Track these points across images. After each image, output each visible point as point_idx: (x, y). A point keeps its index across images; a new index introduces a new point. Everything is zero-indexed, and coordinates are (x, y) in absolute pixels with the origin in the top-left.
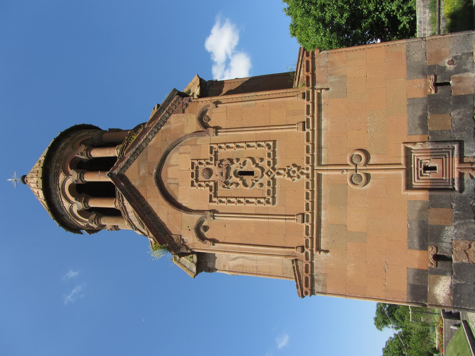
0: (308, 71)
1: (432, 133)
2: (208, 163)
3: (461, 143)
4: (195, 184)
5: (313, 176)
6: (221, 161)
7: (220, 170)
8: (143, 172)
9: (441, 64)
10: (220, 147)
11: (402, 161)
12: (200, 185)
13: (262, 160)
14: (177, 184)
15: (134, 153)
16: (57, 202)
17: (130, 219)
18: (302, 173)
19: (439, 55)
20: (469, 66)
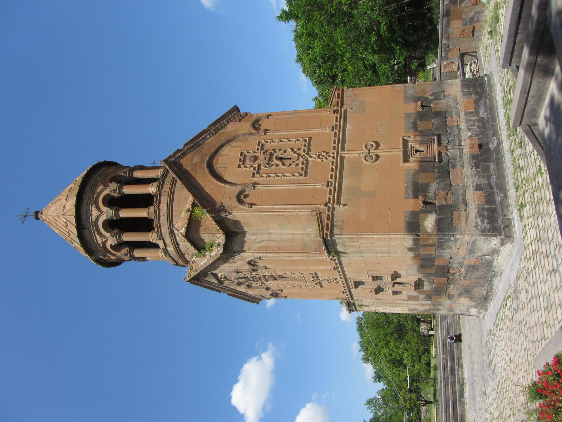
0: (338, 98)
1: (420, 131)
2: (254, 152)
3: (439, 137)
4: (242, 166)
5: (337, 158)
6: (266, 151)
7: (265, 156)
8: (196, 160)
9: (425, 96)
10: (266, 142)
11: (401, 146)
12: (245, 167)
13: (299, 149)
14: (226, 167)
15: (191, 147)
16: (85, 212)
17: (160, 224)
18: (329, 156)
19: (424, 92)
20: (442, 97)
